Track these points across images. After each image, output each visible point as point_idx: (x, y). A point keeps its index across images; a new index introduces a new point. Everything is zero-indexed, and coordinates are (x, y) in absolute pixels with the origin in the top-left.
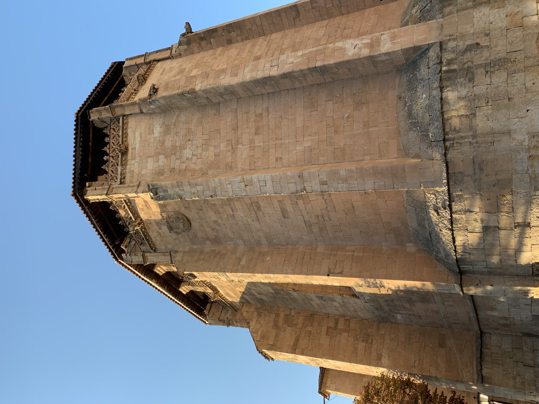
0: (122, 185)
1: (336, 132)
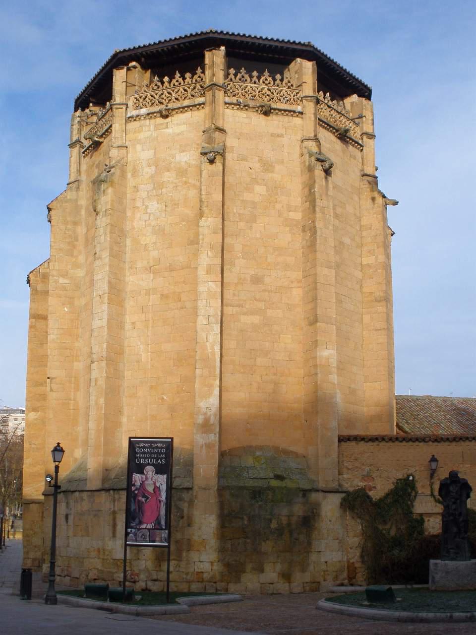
0: (124, 121)
1: (151, 387)
